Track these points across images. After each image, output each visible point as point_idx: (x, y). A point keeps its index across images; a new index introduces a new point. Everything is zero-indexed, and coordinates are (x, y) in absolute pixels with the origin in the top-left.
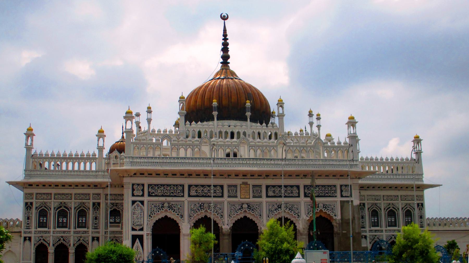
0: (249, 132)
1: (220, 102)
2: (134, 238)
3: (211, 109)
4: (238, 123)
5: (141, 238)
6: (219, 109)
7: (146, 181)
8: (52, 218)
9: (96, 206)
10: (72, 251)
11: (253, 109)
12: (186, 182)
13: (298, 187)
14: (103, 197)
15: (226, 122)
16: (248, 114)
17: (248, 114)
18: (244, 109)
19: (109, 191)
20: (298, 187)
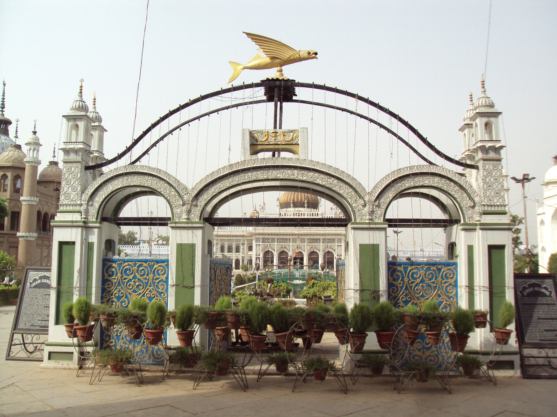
0: (306, 213)
1: (293, 200)
2: (256, 258)
3: (290, 203)
4: (301, 209)
5: (259, 258)
6: (294, 203)
7: (261, 237)
8: (226, 250)
9: (243, 244)
10: (234, 261)
11: (308, 203)
12: (276, 237)
13: (320, 239)
14: (246, 241)
15: (297, 209)
16: (306, 205)
17: (306, 205)
18: (304, 203)
19: (248, 238)
20: (320, 239)
